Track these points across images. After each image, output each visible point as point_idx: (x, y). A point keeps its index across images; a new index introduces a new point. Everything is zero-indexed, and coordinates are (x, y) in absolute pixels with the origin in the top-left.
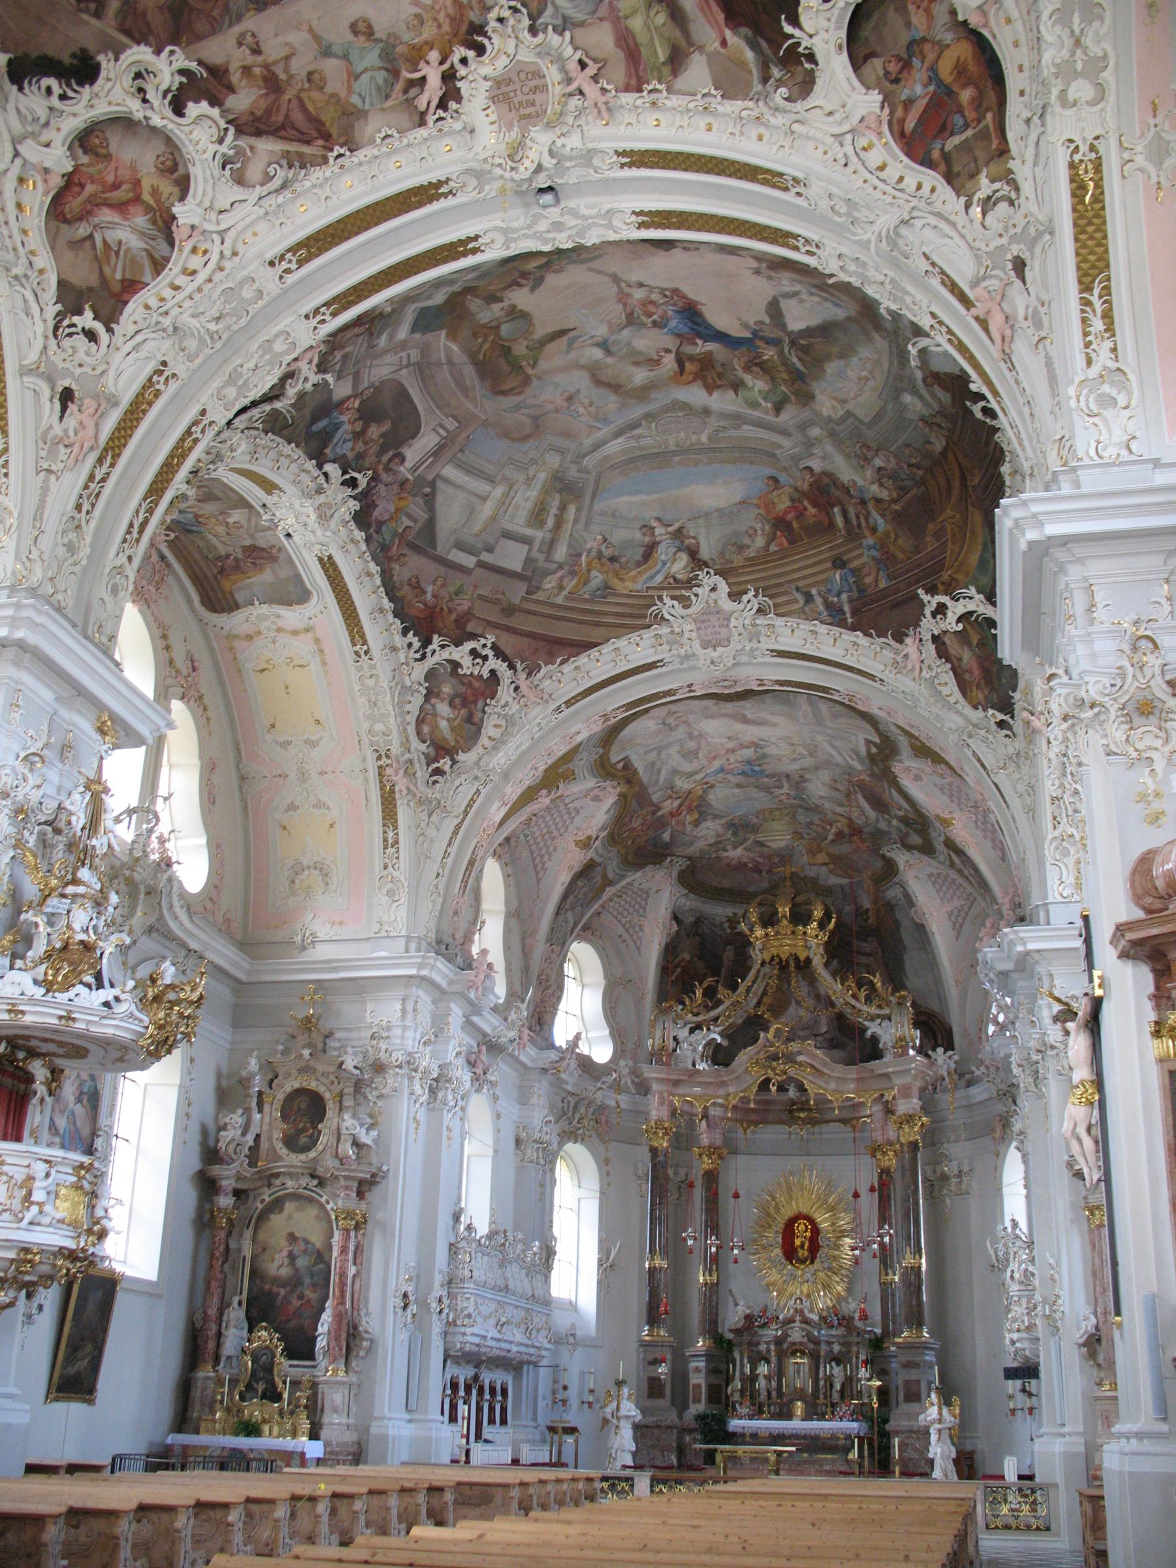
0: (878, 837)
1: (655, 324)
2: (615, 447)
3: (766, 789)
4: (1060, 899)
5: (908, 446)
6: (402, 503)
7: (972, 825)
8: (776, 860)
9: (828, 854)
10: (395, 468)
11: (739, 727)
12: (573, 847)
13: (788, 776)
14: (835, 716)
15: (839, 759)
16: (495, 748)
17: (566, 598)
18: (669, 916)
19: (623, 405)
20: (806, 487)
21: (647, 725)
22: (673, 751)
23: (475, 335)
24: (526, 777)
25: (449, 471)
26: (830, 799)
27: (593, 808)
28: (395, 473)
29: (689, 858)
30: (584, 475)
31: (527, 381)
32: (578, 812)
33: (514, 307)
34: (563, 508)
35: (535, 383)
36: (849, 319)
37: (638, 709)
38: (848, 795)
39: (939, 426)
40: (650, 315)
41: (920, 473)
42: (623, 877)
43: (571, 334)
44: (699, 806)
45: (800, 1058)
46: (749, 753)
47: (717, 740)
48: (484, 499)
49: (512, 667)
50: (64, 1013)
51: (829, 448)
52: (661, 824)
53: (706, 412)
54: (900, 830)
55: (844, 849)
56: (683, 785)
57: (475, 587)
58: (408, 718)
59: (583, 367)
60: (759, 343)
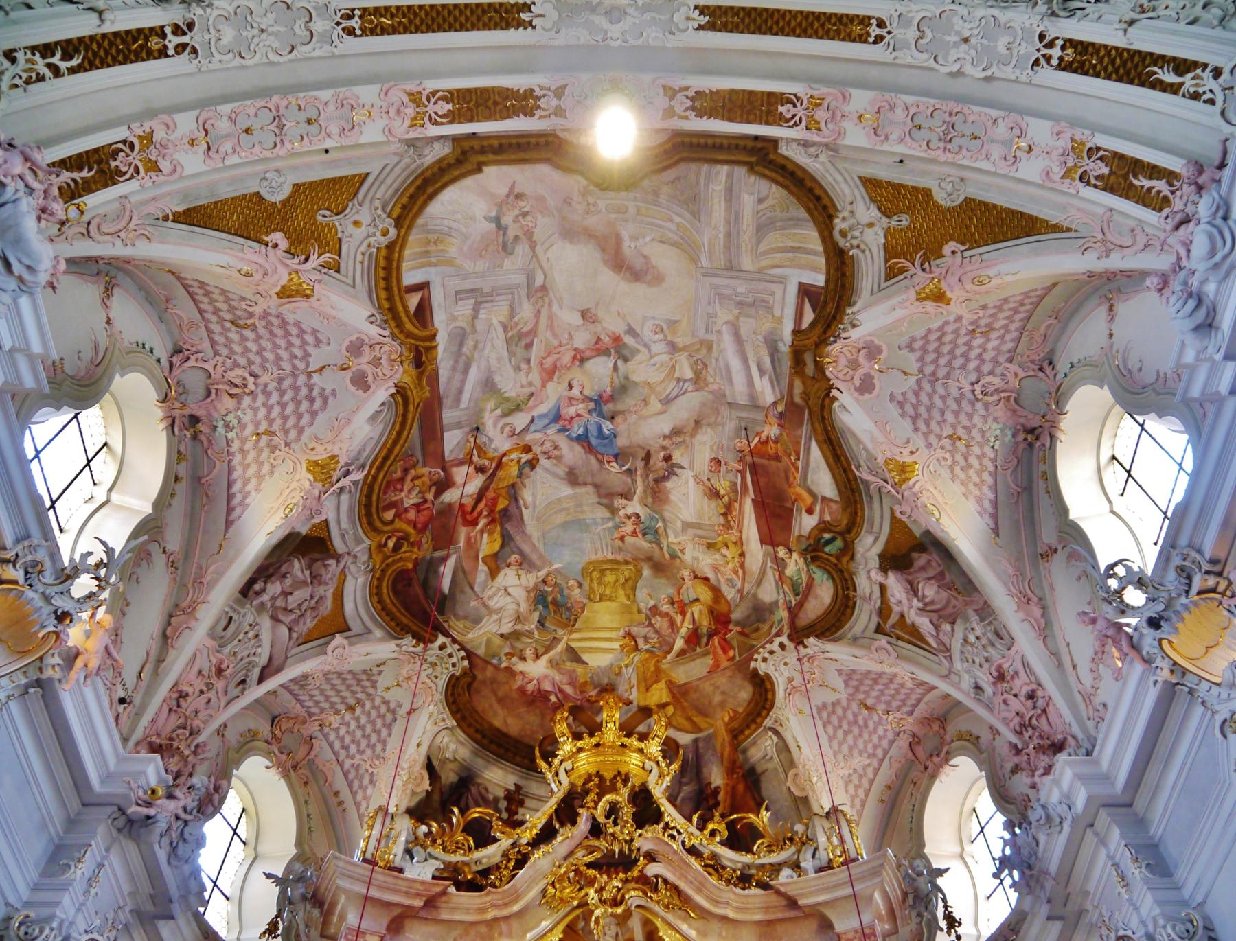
7: (945, 473)
8: (593, 693)
9: (671, 685)
11: (608, 279)
14: (762, 229)
18: (422, 759)
45: (652, 870)
55: (692, 671)
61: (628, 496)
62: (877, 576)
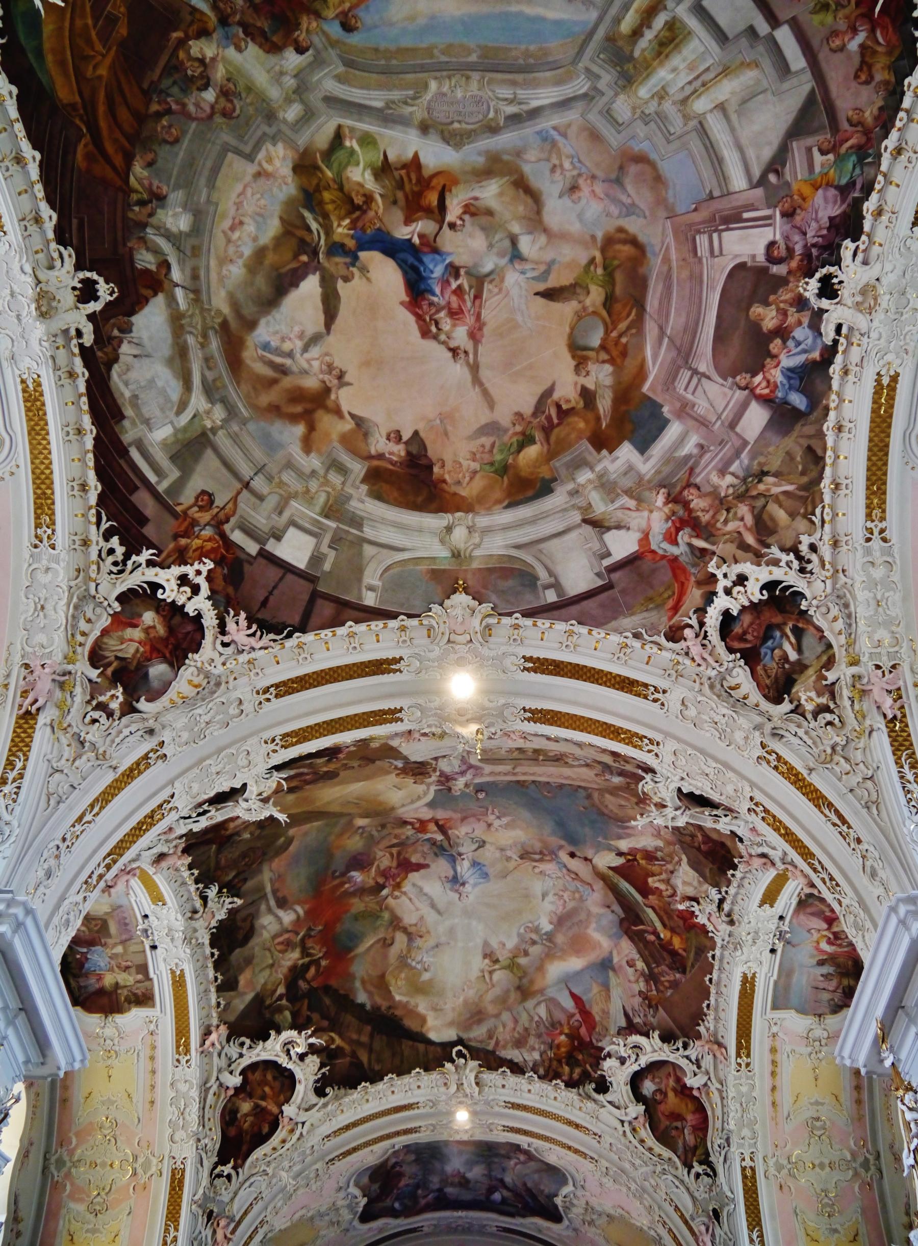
1: (454, 270)
2: (544, 96)
5: (177, 141)
6: (807, 190)
10: (783, 247)
19: (518, 153)
20: (304, 21)
23: (624, 354)
25: (738, 181)
28: (787, 238)
30: (595, 69)
31: (609, 242)
33: (577, 369)
34: (637, 33)
35: (600, 235)
36: (251, 325)
39: (142, 203)
40: (459, 292)
41: (155, 107)
43: (541, 287)
48: (721, 107)
51: (274, 93)
53: (424, 128)
59: (545, 230)
60: (351, 244)
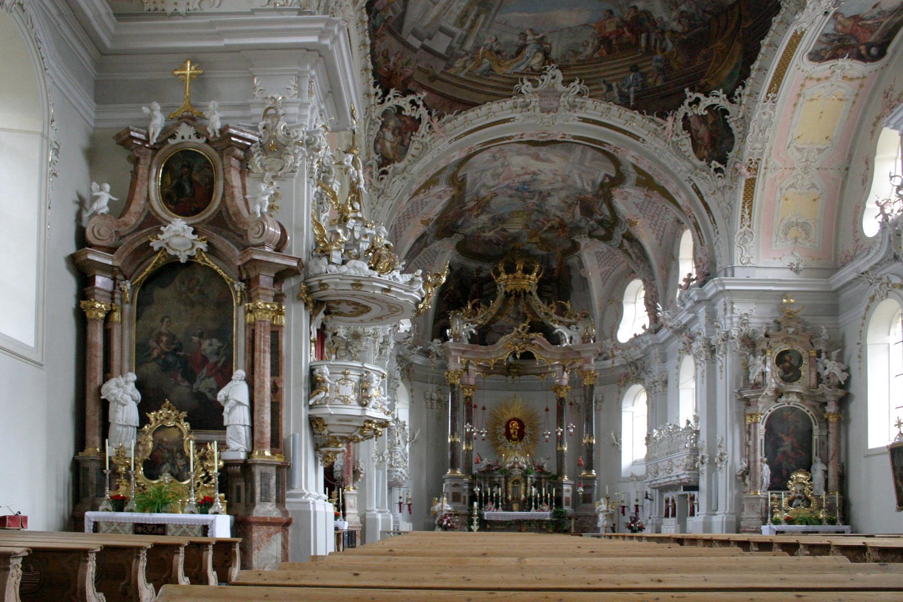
0: (577, 229)
3: (524, 200)
4: (740, 264)
9: (541, 239)
11: (532, 161)
12: (419, 223)
13: (541, 193)
15: (579, 184)
16: (415, 162)
17: (466, 74)
21: (486, 155)
22: (488, 173)
24: (423, 180)
26: (557, 207)
27: (437, 202)
29: (465, 235)
32: (427, 203)
37: (486, 146)
38: (570, 206)
42: (432, 243)
44: (482, 205)
46: (528, 178)
47: (515, 169)
49: (430, 113)
50: (386, 287)
52: (460, 215)
54: (592, 226)
55: (550, 236)
56: (483, 193)
57: (417, 61)
58: (371, 138)
61: (532, 199)
62: (621, 238)
